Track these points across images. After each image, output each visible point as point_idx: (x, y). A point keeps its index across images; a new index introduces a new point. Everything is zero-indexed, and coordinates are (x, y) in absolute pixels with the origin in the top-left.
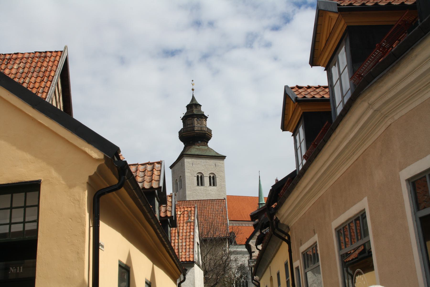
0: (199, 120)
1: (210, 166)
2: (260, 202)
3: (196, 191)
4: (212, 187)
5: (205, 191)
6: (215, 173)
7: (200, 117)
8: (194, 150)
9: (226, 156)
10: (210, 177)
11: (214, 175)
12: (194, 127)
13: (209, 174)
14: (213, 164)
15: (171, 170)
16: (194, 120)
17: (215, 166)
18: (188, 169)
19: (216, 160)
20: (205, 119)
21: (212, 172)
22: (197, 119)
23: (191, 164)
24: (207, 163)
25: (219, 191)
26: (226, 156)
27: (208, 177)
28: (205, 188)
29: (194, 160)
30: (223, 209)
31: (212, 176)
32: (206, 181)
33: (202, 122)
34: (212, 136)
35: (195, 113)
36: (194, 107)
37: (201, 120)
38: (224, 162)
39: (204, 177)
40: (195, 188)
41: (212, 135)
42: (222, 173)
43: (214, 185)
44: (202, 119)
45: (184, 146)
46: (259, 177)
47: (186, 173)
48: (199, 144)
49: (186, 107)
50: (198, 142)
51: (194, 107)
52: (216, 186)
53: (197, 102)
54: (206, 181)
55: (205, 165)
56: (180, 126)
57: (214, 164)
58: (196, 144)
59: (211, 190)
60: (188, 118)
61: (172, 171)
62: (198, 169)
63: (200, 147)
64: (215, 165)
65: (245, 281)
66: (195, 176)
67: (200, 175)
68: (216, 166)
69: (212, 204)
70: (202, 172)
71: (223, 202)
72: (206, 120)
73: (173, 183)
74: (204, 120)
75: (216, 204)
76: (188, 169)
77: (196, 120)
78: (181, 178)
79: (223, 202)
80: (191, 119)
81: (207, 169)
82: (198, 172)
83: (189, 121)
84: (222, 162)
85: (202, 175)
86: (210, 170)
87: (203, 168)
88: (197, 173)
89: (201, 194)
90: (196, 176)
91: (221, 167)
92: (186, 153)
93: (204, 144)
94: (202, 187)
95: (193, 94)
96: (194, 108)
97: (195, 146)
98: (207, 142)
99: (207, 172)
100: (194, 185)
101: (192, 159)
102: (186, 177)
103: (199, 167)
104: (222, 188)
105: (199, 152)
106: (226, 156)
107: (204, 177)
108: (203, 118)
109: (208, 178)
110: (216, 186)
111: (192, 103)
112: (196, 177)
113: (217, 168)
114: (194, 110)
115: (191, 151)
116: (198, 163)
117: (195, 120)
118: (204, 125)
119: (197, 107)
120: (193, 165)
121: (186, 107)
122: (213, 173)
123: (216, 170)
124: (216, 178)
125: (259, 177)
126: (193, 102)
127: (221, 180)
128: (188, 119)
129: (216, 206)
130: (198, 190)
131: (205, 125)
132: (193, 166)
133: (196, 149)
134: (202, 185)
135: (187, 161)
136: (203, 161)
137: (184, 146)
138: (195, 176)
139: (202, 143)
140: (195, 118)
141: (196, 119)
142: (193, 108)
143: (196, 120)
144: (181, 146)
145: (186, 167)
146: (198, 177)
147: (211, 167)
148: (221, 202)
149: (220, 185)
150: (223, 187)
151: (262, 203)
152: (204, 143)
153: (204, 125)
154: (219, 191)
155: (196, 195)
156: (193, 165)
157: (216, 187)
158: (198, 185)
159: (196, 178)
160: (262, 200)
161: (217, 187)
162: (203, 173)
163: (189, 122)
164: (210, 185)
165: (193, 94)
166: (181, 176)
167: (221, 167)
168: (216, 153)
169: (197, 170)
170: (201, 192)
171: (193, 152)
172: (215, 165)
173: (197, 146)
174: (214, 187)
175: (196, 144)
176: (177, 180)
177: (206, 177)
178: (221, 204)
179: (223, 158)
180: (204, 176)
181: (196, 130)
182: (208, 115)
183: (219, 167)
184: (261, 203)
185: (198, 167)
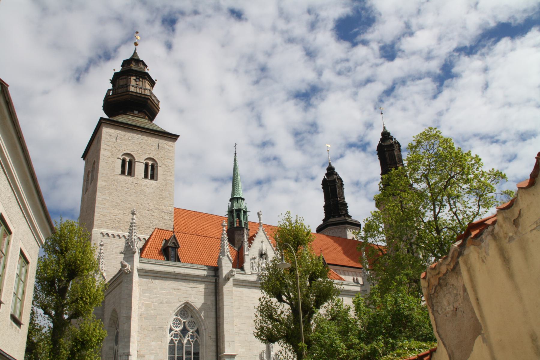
0: (140, 81)
1: (149, 146)
2: (234, 196)
3: (117, 183)
4: (149, 182)
5: (134, 186)
6: (157, 160)
7: (141, 76)
11: (154, 163)
12: (129, 87)
13: (146, 159)
14: (154, 144)
16: (130, 78)
17: (157, 147)
18: (108, 145)
19: (161, 139)
21: (152, 157)
22: (137, 78)
23: (114, 137)
24: (144, 141)
25: (160, 189)
27: (142, 164)
28: (135, 181)
29: (120, 132)
31: (150, 163)
32: (139, 169)
33: (143, 83)
37: (142, 81)
38: (174, 144)
39: (136, 163)
40: (116, 177)
41: (159, 108)
42: (169, 161)
43: (153, 178)
44: (144, 80)
46: (235, 154)
47: (102, 150)
48: (134, 114)
50: (133, 112)
52: (157, 180)
53: (139, 58)
54: (139, 169)
55: (139, 143)
57: (157, 145)
59: (145, 185)
60: (121, 76)
62: (125, 148)
64: (158, 146)
65: (192, 341)
66: (118, 158)
67: (129, 159)
68: (159, 149)
70: (132, 153)
76: (108, 145)
77: (133, 79)
80: (126, 78)
81: (143, 150)
82: (125, 152)
83: (122, 80)
84: (171, 145)
85: (133, 159)
86: (148, 153)
87: (136, 148)
88: (122, 153)
89: (127, 189)
90: (120, 157)
91: (169, 151)
94: (130, 178)
99: (142, 155)
100: (115, 173)
101: (117, 131)
102: (101, 156)
103: (128, 144)
104: (166, 185)
107: (135, 162)
108: (146, 79)
109: (143, 166)
110: (157, 180)
112: (121, 161)
113: (160, 152)
116: (127, 137)
117: (132, 79)
120: (116, 140)
122: (153, 158)
123: (158, 154)
124: (157, 167)
125: (235, 154)
127: (166, 173)
128: (120, 78)
130: (122, 182)
132: (117, 141)
136: (136, 136)
138: (118, 158)
140: (133, 76)
141: (134, 78)
143: (133, 79)
145: (104, 141)
146: (124, 161)
147: (149, 148)
149: (163, 180)
150: (169, 183)
151: (239, 196)
152: (143, 115)
154: (160, 189)
155: (116, 189)
156: (116, 140)
157: (155, 181)
158: (123, 173)
159: (120, 162)
160: (238, 193)
161: (157, 182)
162: (134, 156)
163: (121, 82)
164: (146, 176)
167: (169, 151)
169: (123, 149)
170: (127, 186)
172: (158, 146)
174: (153, 181)
177: (139, 163)
179: (174, 137)
180: (135, 159)
182: (156, 80)
183: (164, 151)
184: (235, 196)
185: (125, 145)
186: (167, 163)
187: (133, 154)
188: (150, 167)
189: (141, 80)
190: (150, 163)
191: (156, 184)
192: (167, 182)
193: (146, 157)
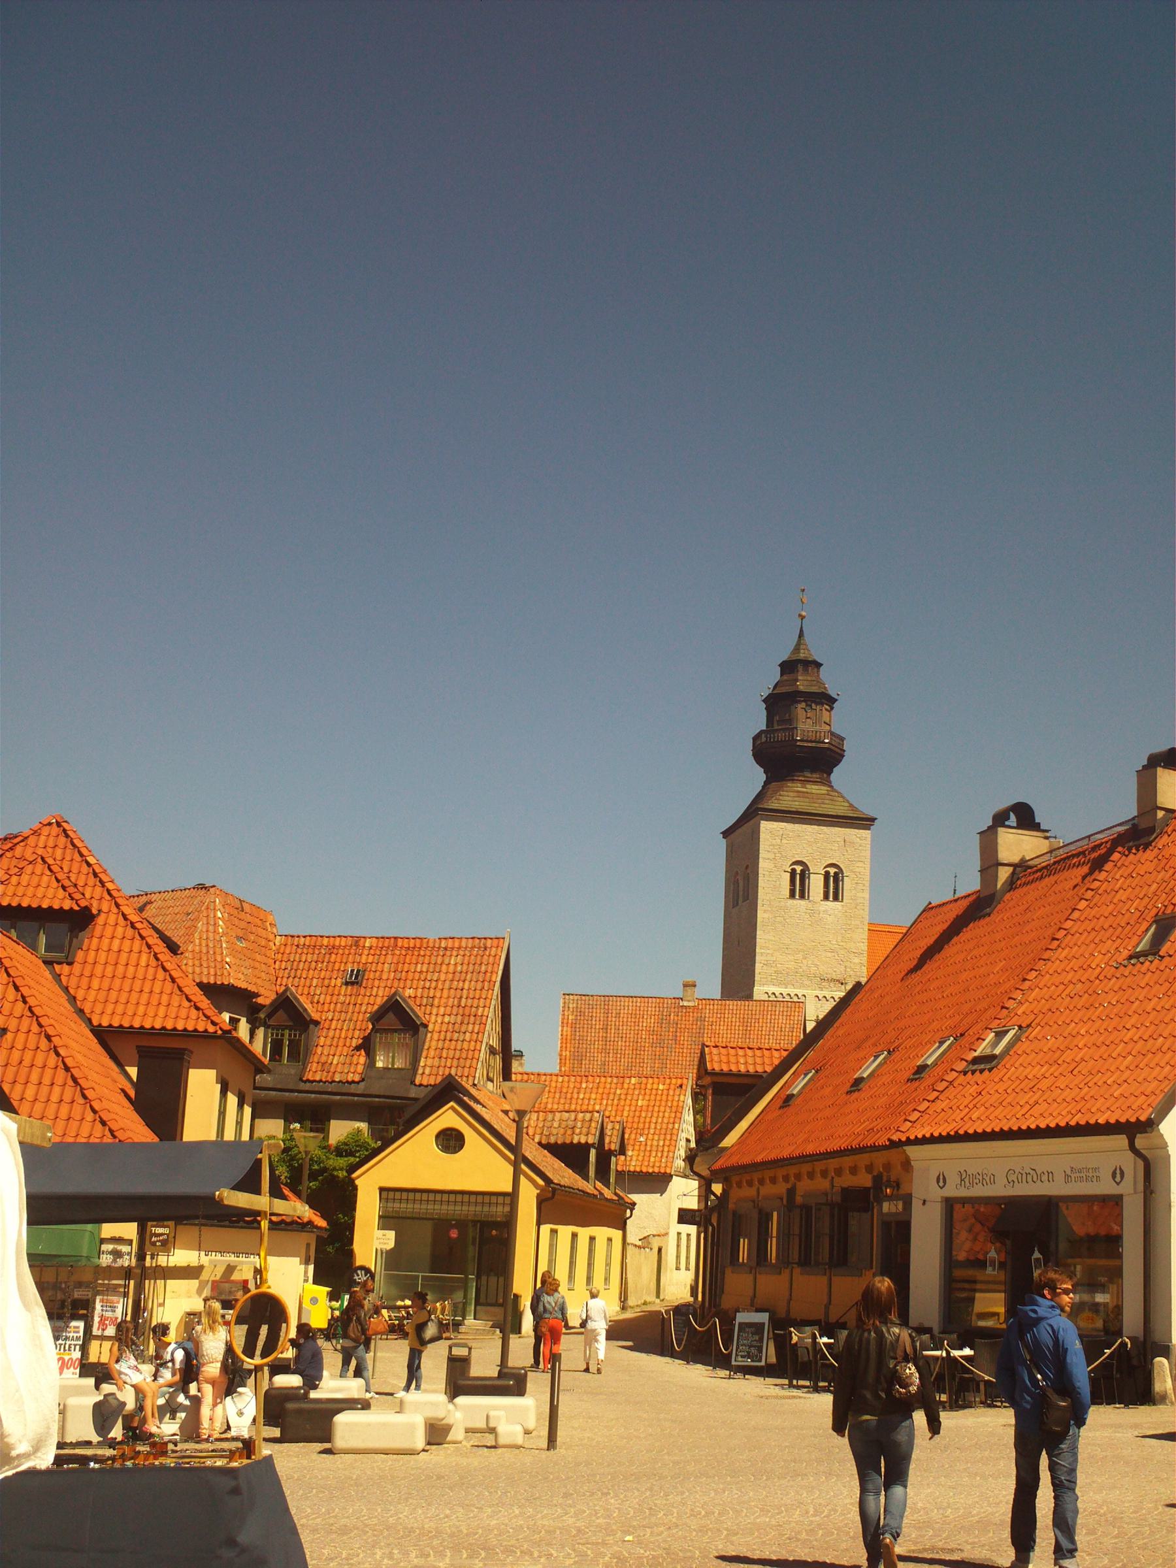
4: (831, 904)
8: (790, 797)
9: (876, 819)
10: (827, 875)
13: (825, 868)
15: (725, 840)
20: (827, 705)
21: (834, 862)
22: (807, 705)
26: (875, 816)
28: (810, 905)
30: (796, 1026)
31: (832, 871)
32: (816, 884)
34: (846, 754)
35: (801, 688)
36: (800, 668)
39: (811, 875)
41: (844, 751)
43: (836, 898)
45: (765, 779)
47: (761, 860)
49: (780, 665)
51: (800, 668)
54: (816, 884)
56: (758, 721)
58: (796, 778)
59: (825, 911)
61: (727, 846)
63: (808, 786)
69: (773, 1013)
71: (797, 1009)
72: (832, 708)
73: (727, 880)
74: (826, 710)
75: (781, 1014)
78: (749, 871)
79: (797, 1009)
82: (794, 860)
88: (791, 862)
92: (766, 807)
93: (819, 778)
94: (802, 902)
95: (801, 627)
96: (800, 673)
97: (793, 785)
98: (830, 773)
102: (760, 871)
104: (856, 908)
105: (802, 804)
106: (876, 819)
107: (809, 874)
109: (822, 878)
111: (795, 658)
112: (789, 874)
114: (800, 678)
115: (781, 797)
118: (825, 722)
119: (810, 670)
121: (780, 665)
126: (799, 653)
129: (781, 1017)
131: (828, 721)
133: (795, 794)
134: (802, 896)
135: (769, 830)
137: (764, 777)
139: (814, 776)
140: (800, 702)
141: (803, 705)
142: (798, 671)
144: (758, 776)
146: (793, 872)
148: (793, 1009)
153: (825, 722)
165: (801, 627)
166: (747, 867)
168: (850, 808)
171: (786, 802)
173: (799, 785)
174: (836, 903)
175: (796, 778)
176: (737, 873)
178: (793, 1014)
180: (809, 870)
181: (798, 738)
182: (838, 695)
186: (857, 870)
187: (806, 862)
188: (832, 878)
189: (814, 706)
190: (832, 871)
191: (840, 908)
192: (858, 901)
193: (826, 864)
